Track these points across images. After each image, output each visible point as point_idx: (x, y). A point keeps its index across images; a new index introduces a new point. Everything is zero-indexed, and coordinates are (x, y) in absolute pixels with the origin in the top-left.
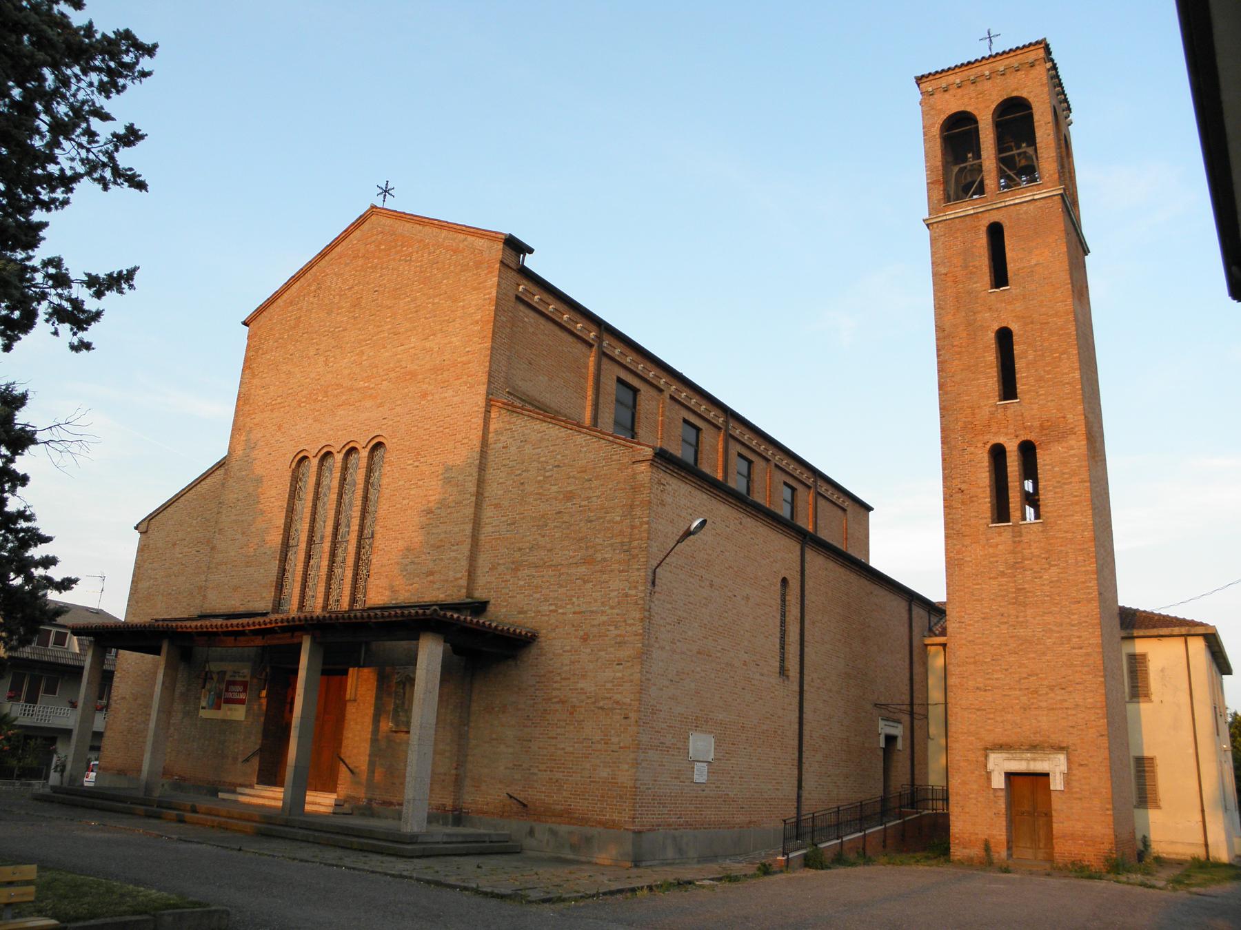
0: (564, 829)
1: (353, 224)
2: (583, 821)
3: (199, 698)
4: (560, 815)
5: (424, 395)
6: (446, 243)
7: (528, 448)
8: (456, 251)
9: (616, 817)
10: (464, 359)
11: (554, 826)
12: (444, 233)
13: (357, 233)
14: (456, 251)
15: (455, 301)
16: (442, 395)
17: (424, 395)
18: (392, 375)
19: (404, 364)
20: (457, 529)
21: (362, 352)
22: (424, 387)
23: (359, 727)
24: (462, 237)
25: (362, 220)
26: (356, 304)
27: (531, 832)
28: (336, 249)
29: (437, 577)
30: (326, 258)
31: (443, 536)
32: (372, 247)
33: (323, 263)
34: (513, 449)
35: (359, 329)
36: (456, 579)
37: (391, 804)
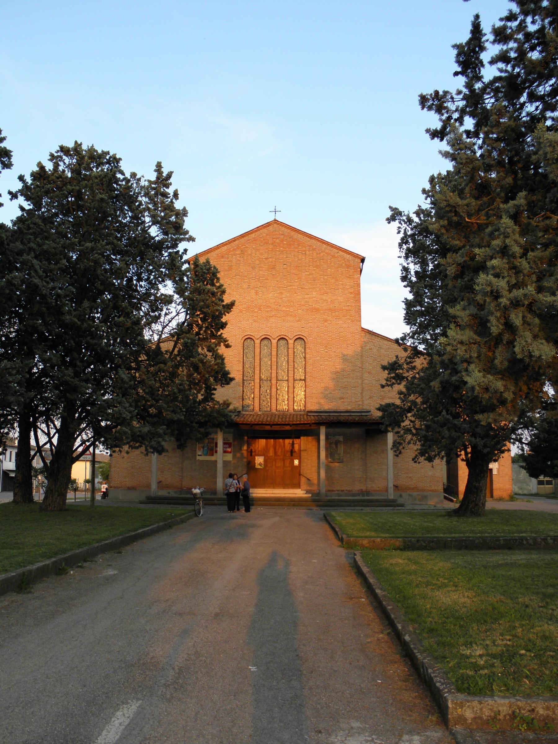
0: (415, 494)
1: (262, 225)
2: (423, 490)
3: (196, 451)
4: (413, 489)
5: (326, 321)
6: (327, 251)
7: (382, 351)
8: (333, 257)
9: (436, 488)
10: (346, 308)
11: (411, 493)
12: (324, 246)
13: (265, 230)
14: (333, 257)
15: (337, 280)
16: (338, 322)
17: (326, 321)
18: (304, 308)
19: (311, 304)
20: (354, 381)
21: (281, 293)
22: (325, 317)
23: (309, 461)
24: (337, 251)
25: (268, 225)
26: (274, 268)
27: (401, 496)
28: (251, 235)
29: (345, 400)
30: (245, 238)
31: (346, 383)
32: (278, 241)
33: (243, 240)
34: (375, 350)
35: (277, 281)
36: (357, 401)
37: (333, 491)
